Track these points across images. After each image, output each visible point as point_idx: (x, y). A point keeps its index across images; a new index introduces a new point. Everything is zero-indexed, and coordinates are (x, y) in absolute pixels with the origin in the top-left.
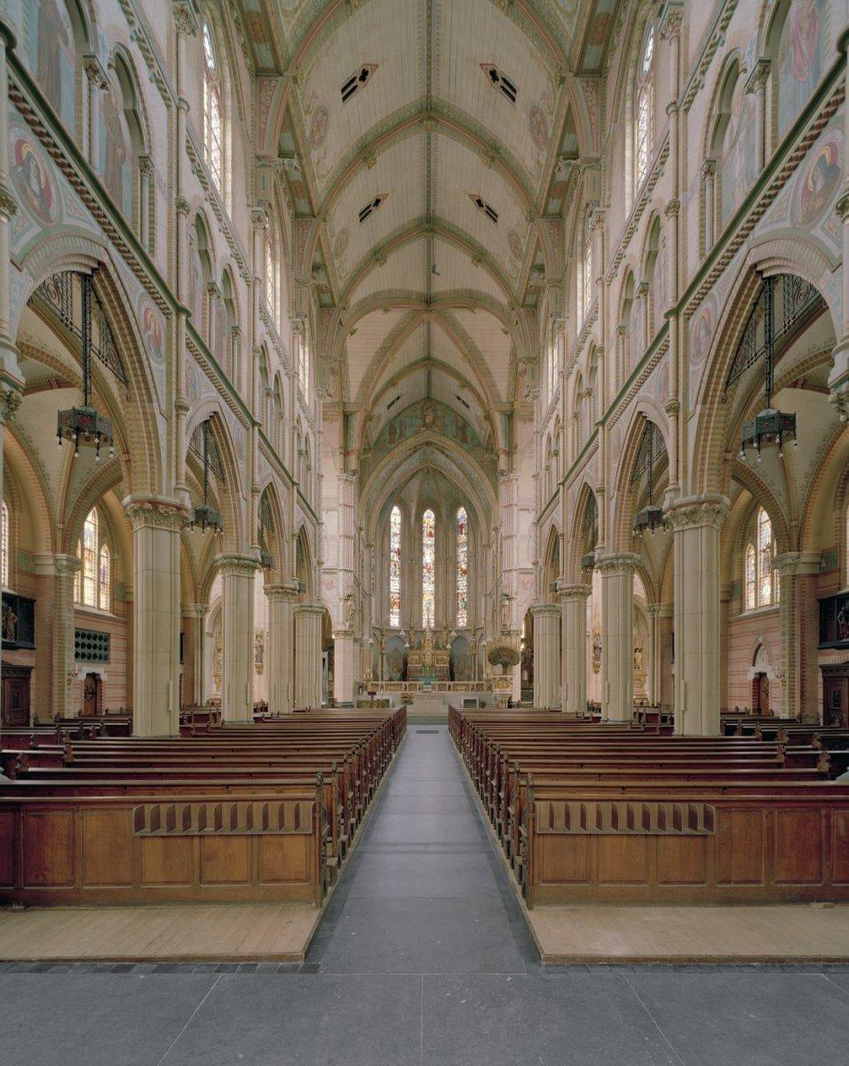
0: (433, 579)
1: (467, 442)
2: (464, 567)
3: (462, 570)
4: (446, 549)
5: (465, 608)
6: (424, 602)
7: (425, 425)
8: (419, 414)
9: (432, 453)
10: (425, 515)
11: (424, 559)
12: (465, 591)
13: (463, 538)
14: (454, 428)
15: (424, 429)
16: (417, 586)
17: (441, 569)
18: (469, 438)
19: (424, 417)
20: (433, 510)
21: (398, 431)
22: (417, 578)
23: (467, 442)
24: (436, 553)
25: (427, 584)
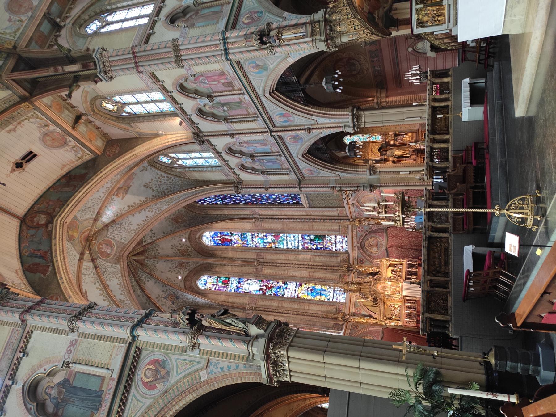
0: (281, 284)
1: (86, 174)
2: (270, 238)
3: (273, 242)
4: (246, 262)
5: (323, 237)
6: (310, 297)
7: (46, 225)
8: (32, 232)
9: (109, 244)
10: (202, 287)
11: (253, 292)
12: (300, 236)
13: (236, 238)
14: (66, 189)
15: (50, 226)
16: (286, 305)
17: (268, 271)
18: (83, 172)
19: (38, 226)
20: (198, 278)
21: (38, 260)
22: (275, 304)
23: (86, 174)
24: (249, 276)
25: (286, 291)
